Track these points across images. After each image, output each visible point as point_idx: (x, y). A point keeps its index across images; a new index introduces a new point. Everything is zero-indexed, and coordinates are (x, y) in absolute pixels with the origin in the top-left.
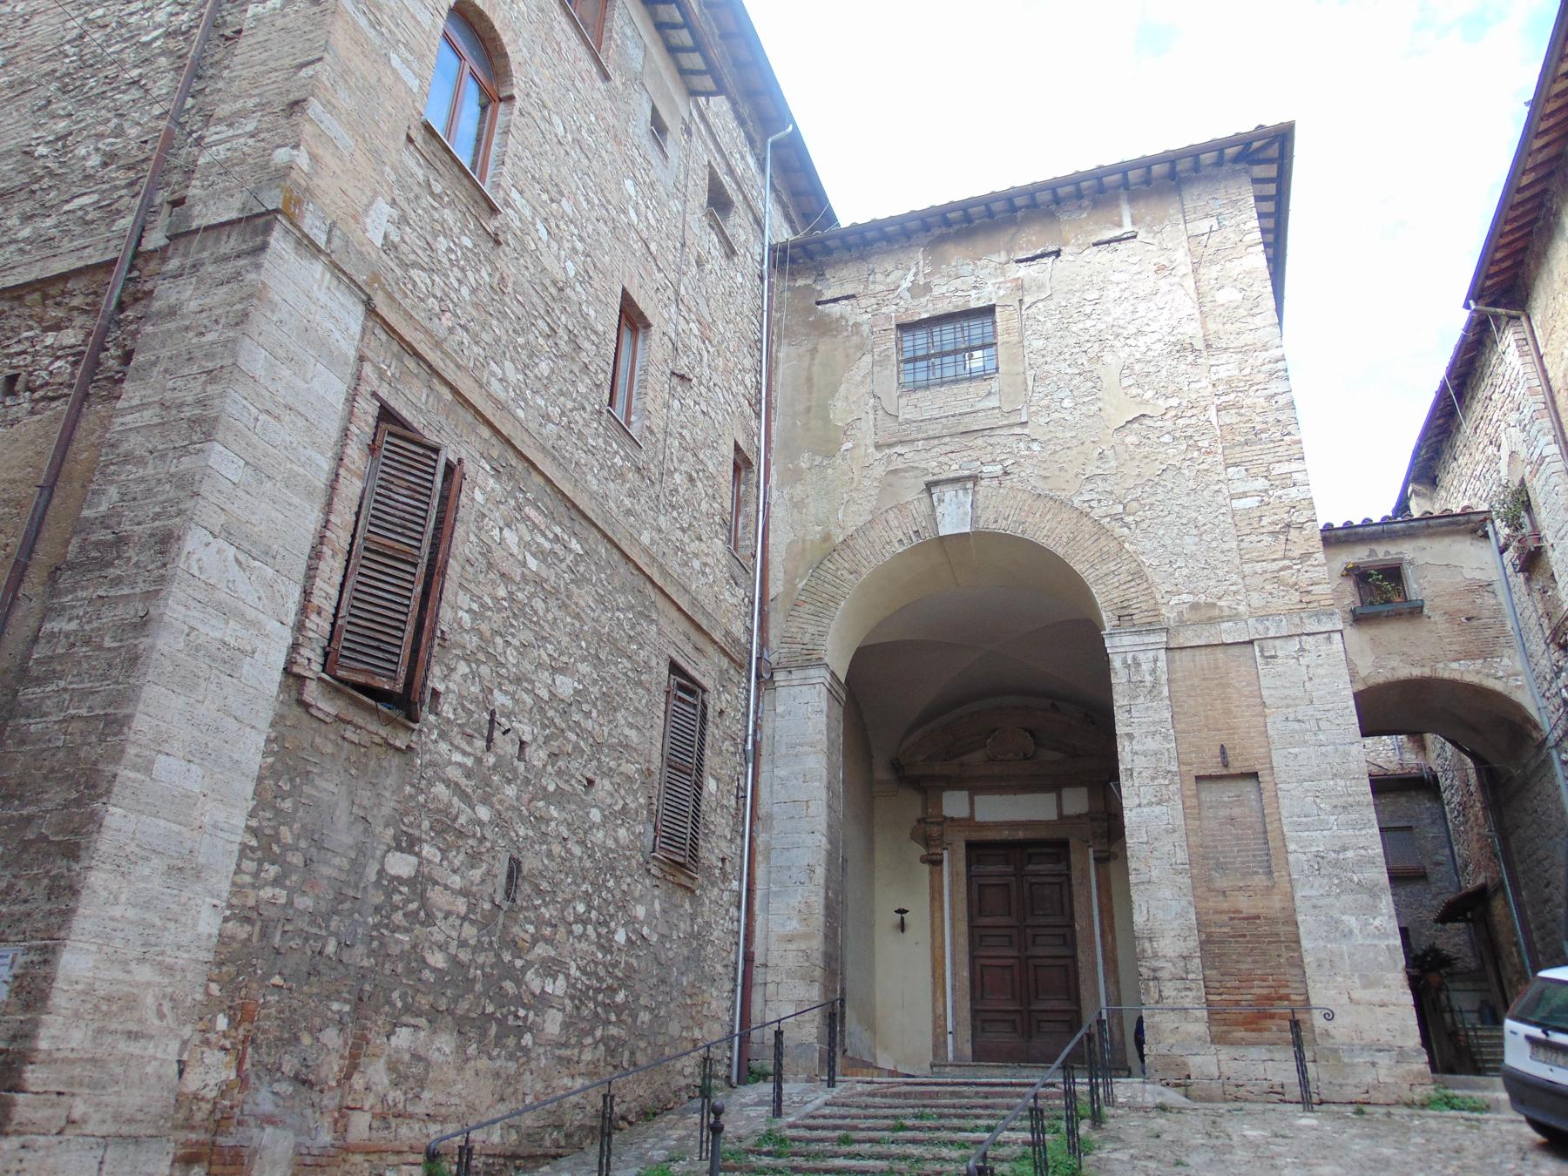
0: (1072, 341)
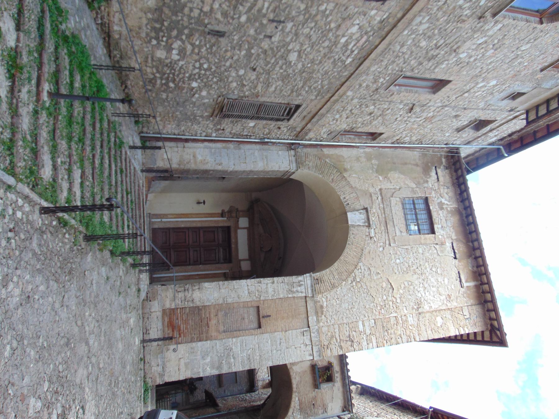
0: (421, 263)
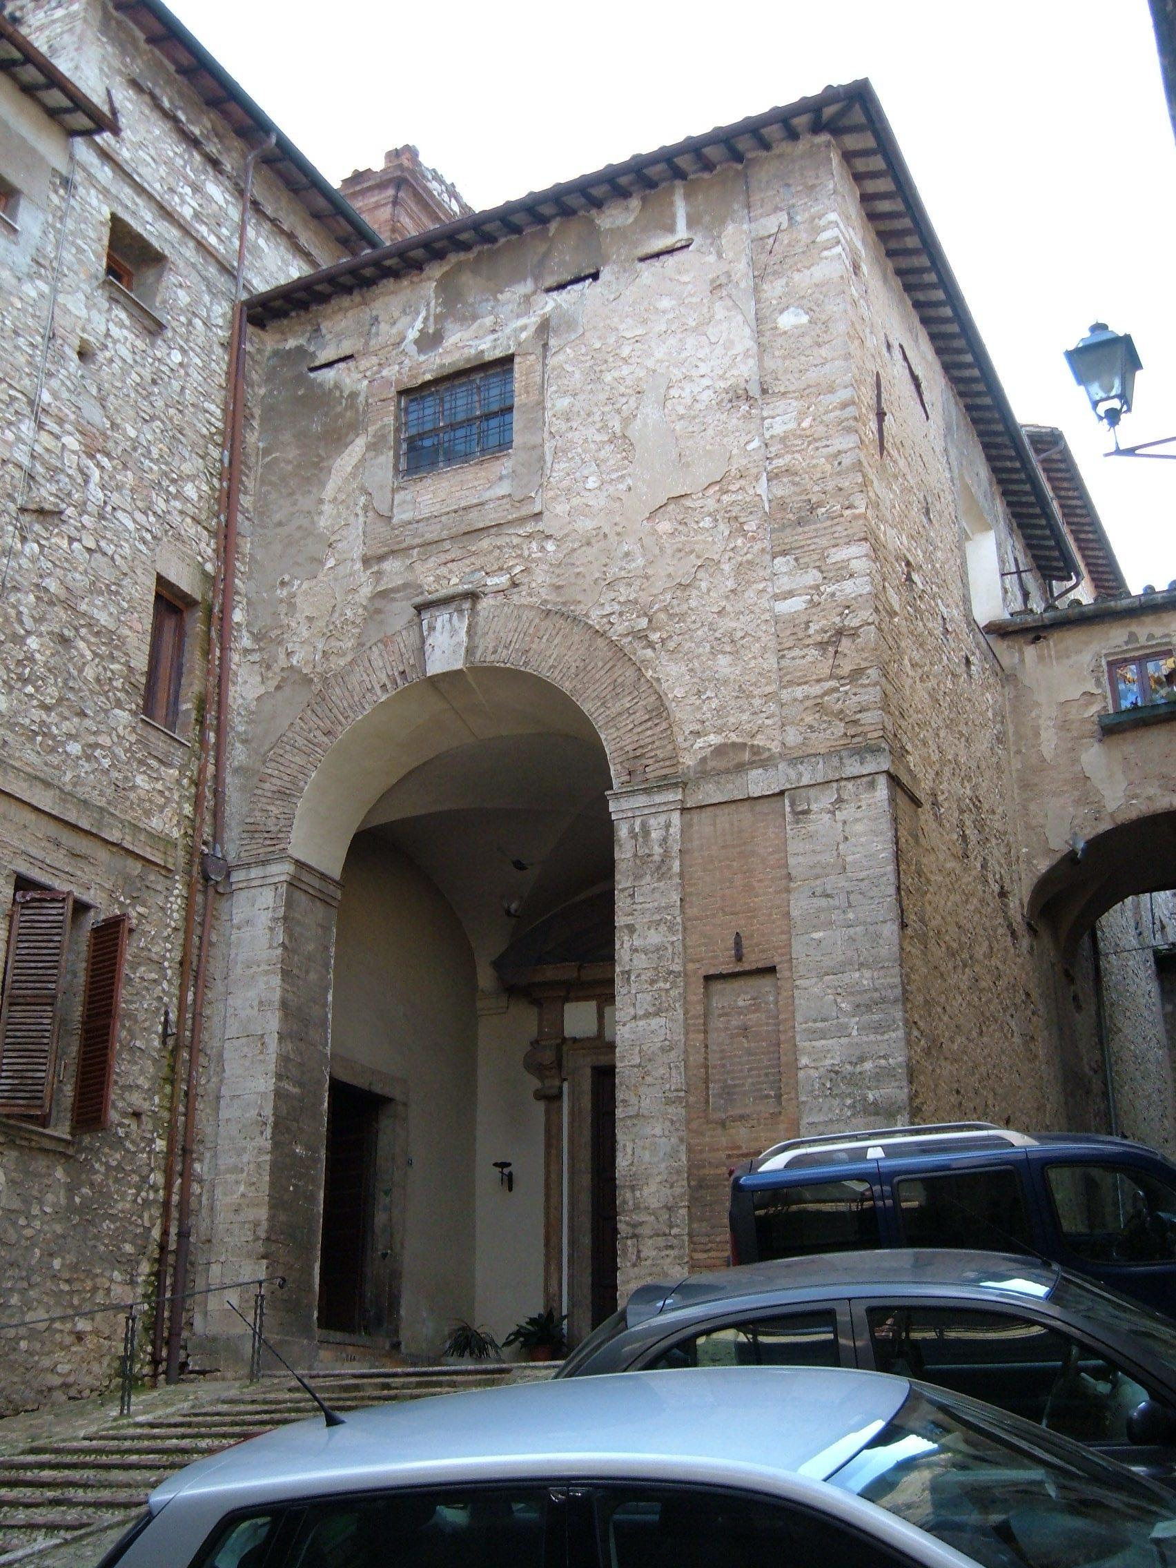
0: (602, 397)
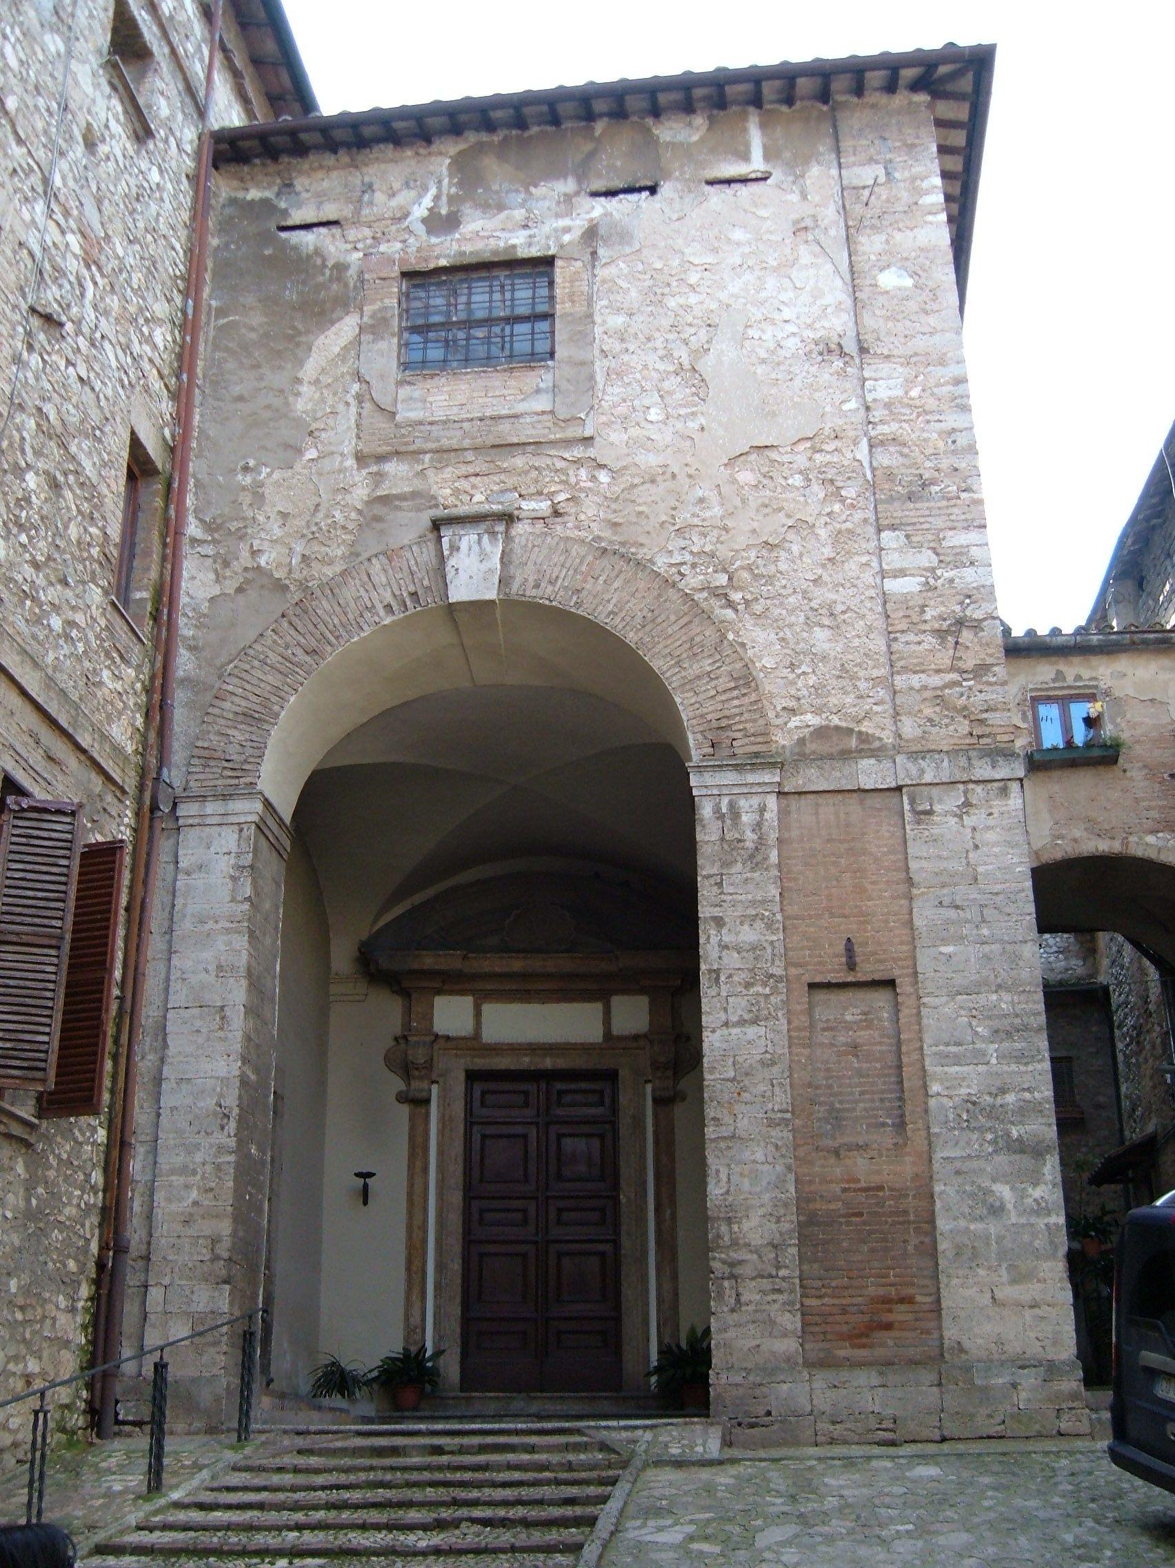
0: (666, 322)
